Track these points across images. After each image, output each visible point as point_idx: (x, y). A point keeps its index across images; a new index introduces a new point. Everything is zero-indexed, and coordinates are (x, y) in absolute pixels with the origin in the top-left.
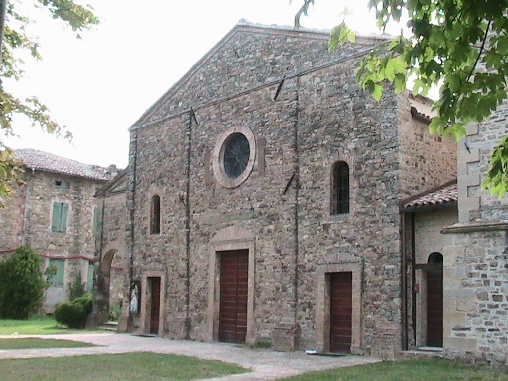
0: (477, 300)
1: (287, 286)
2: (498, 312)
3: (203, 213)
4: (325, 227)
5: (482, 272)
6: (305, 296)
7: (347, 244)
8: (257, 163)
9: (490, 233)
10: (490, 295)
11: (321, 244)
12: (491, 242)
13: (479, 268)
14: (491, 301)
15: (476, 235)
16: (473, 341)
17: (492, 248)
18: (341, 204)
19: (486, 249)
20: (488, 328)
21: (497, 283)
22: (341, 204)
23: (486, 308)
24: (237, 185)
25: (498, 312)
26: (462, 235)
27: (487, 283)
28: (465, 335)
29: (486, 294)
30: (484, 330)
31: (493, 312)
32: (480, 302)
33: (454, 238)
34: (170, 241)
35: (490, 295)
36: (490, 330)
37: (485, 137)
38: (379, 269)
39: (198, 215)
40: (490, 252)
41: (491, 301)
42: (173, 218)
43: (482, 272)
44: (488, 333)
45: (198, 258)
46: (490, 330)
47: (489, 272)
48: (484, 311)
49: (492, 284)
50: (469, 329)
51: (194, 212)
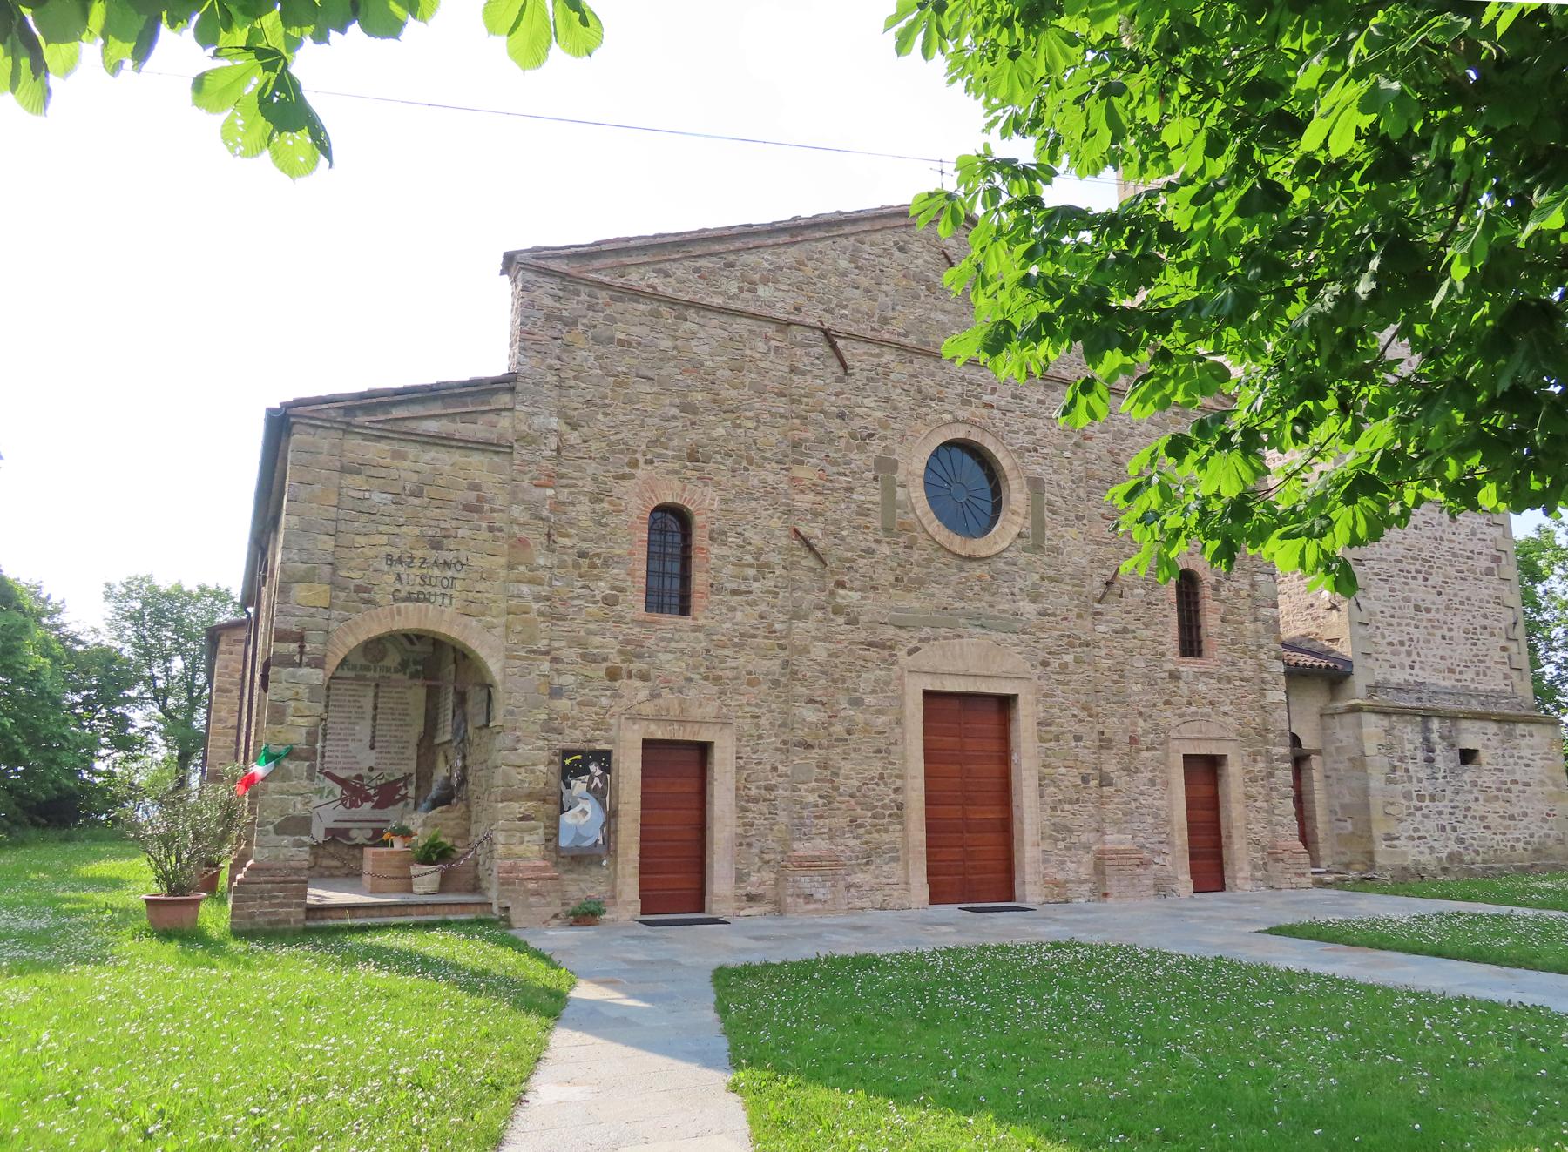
0: (1403, 801)
1: (1112, 775)
2: (1424, 816)
3: (871, 594)
4: (1174, 676)
5: (1404, 766)
6: (1142, 794)
7: (1208, 709)
8: (1028, 523)
9: (1408, 718)
10: (1415, 794)
11: (1167, 703)
12: (1409, 729)
13: (1401, 760)
14: (1415, 802)
15: (1394, 718)
16: (1405, 853)
17: (1410, 736)
18: (1191, 644)
19: (1405, 736)
20: (1416, 835)
21: (1420, 780)
22: (1191, 644)
23: (1412, 810)
24: (983, 554)
25: (1424, 816)
26: (1381, 717)
27: (1410, 778)
28: (1395, 846)
29: (1410, 792)
30: (1413, 839)
31: (1418, 814)
32: (1406, 803)
33: (1373, 718)
34: (741, 646)
35: (1415, 794)
36: (1419, 838)
37: (1371, 595)
38: (1258, 753)
39: (855, 596)
40: (1411, 742)
41: (1415, 802)
42: (756, 585)
43: (1404, 766)
44: (1417, 842)
45: (856, 702)
46: (1419, 838)
47: (1411, 767)
48: (1409, 814)
49: (1415, 780)
50: (1398, 838)
51: (840, 584)
